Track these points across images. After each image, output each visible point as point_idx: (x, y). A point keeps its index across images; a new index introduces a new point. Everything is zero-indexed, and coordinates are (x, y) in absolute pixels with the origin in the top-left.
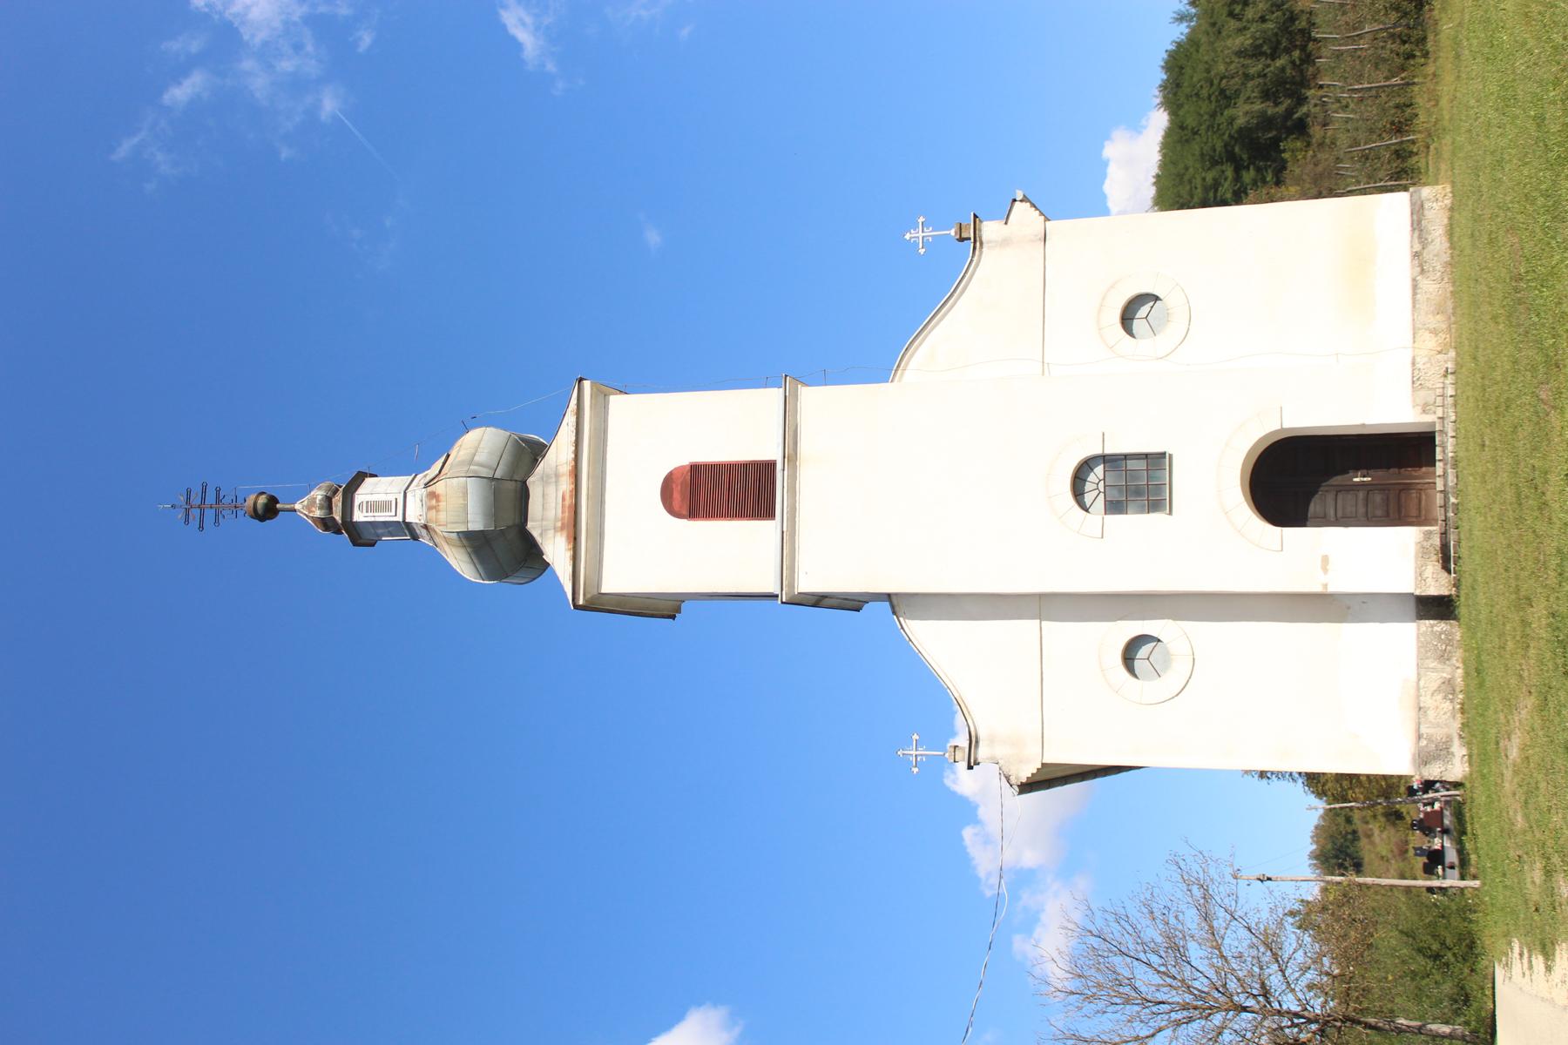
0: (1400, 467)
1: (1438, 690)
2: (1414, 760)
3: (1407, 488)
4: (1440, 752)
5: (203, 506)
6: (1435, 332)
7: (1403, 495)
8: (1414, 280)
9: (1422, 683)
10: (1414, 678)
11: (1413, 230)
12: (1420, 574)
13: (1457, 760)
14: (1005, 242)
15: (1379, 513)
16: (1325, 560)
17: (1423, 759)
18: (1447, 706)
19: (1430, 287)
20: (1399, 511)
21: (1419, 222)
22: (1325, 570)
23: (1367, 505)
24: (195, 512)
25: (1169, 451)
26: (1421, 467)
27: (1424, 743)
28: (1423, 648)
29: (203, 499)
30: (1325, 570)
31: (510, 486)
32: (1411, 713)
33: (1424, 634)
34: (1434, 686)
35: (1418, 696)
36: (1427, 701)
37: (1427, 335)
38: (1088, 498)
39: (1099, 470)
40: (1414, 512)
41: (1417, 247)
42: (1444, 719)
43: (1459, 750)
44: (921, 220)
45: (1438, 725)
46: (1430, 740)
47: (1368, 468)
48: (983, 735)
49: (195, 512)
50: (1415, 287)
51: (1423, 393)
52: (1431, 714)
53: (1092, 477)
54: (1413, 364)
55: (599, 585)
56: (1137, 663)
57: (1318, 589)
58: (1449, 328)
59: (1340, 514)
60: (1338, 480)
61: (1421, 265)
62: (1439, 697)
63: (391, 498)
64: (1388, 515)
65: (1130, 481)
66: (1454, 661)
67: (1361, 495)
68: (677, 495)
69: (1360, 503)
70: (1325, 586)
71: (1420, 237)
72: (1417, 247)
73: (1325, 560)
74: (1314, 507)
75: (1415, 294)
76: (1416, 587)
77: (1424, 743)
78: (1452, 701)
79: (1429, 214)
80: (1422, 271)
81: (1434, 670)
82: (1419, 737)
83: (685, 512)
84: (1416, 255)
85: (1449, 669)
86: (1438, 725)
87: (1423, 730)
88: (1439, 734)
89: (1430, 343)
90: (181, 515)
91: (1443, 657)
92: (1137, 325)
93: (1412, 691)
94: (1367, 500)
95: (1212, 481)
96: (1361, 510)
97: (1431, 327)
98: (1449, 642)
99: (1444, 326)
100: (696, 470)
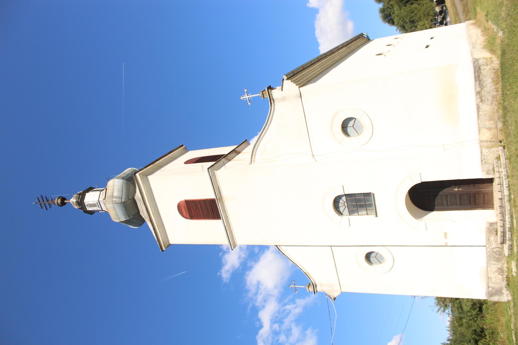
4: (499, 292)
5: (44, 202)
6: (489, 129)
8: (478, 105)
9: (489, 269)
10: (485, 266)
11: (476, 80)
12: (488, 240)
13: (505, 295)
14: (284, 99)
16: (446, 234)
17: (491, 294)
18: (500, 277)
19: (486, 108)
20: (475, 202)
21: (479, 77)
22: (446, 238)
23: (461, 200)
24: (43, 205)
25: (372, 192)
27: (490, 289)
29: (44, 201)
30: (446, 238)
31: (130, 202)
33: (489, 252)
34: (495, 270)
36: (491, 275)
37: (485, 131)
38: (341, 209)
39: (344, 198)
41: (478, 89)
43: (505, 291)
44: (246, 90)
45: (496, 283)
46: (493, 288)
48: (317, 283)
49: (43, 205)
50: (478, 108)
52: (493, 280)
53: (341, 201)
54: (481, 153)
55: (168, 242)
56: (371, 259)
58: (497, 127)
59: (449, 203)
61: (481, 98)
62: (497, 274)
63: (96, 203)
64: (470, 203)
65: (359, 203)
66: (503, 261)
67: (458, 196)
68: (184, 211)
71: (479, 84)
72: (478, 89)
73: (446, 234)
74: (437, 201)
75: (478, 112)
77: (490, 289)
78: (502, 275)
79: (483, 72)
80: (482, 101)
81: (494, 264)
82: (489, 287)
83: (189, 217)
84: (478, 93)
85: (500, 264)
86: (496, 283)
87: (490, 285)
88: (497, 286)
90: (39, 206)
92: (350, 130)
95: (393, 199)
96: (458, 202)
97: (488, 127)
99: (494, 126)
100: (187, 202)
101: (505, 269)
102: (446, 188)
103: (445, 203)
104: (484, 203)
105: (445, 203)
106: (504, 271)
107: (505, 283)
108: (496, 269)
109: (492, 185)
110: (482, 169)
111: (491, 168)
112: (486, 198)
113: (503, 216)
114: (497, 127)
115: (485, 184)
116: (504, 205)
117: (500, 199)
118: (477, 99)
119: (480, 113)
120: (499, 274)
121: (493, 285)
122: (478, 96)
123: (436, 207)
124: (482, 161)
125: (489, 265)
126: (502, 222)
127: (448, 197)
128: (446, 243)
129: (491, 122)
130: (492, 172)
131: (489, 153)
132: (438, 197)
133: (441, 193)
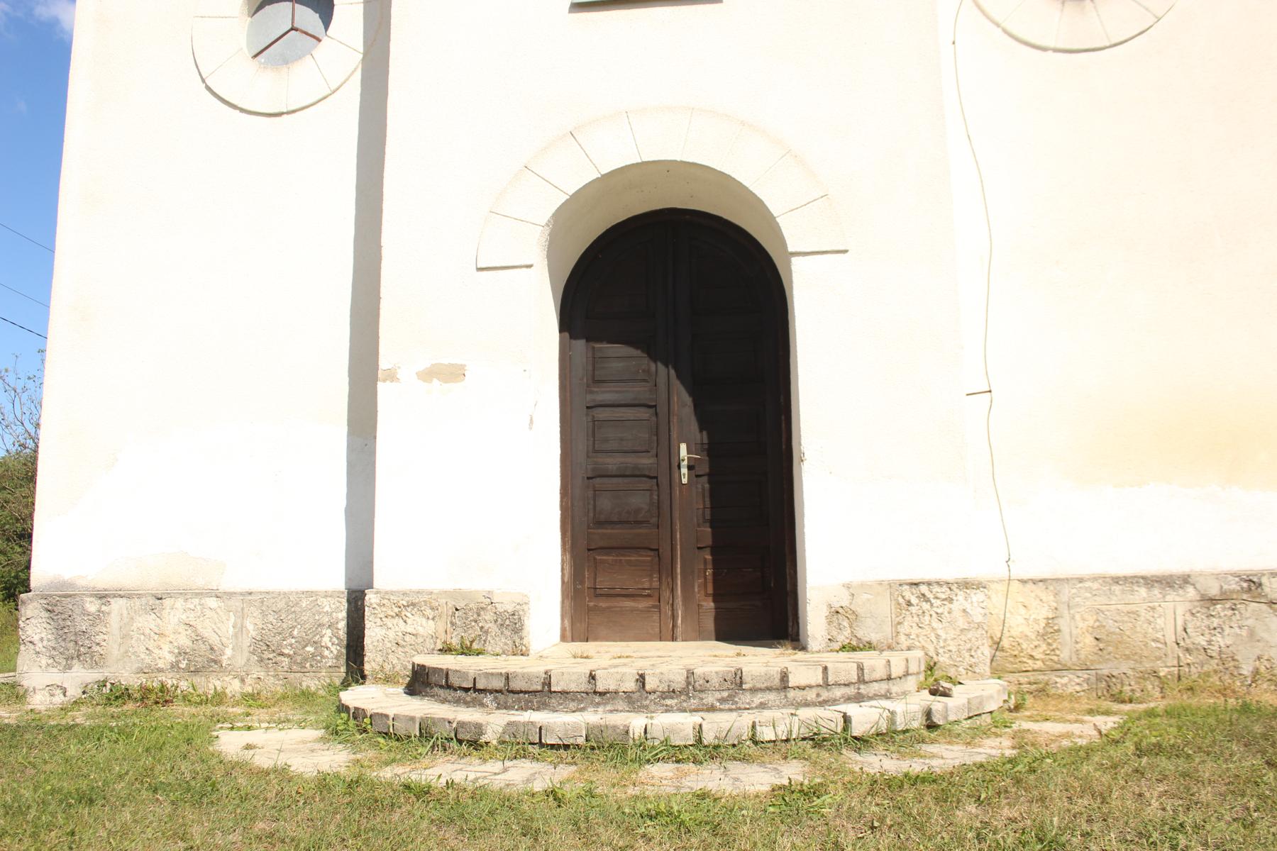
0: (714, 550)
1: (198, 638)
2: (64, 585)
3: (663, 567)
4: (74, 643)
6: (1050, 631)
7: (646, 557)
8: (1186, 580)
9: (212, 602)
10: (233, 581)
12: (410, 604)
13: (56, 677)
15: (605, 503)
16: (454, 373)
17: (60, 606)
18: (165, 656)
19: (1169, 617)
22: (429, 374)
26: (717, 597)
27: (92, 606)
28: (282, 608)
30: (429, 374)
32: (154, 582)
34: (207, 631)
35: (185, 594)
36: (175, 613)
37: (1044, 613)
40: (604, 582)
42: (138, 649)
43: (78, 678)
46: (99, 617)
47: (711, 475)
50: (1167, 582)
51: (885, 607)
52: (147, 622)
54: (966, 585)
57: (384, 363)
58: (1061, 669)
59: (603, 414)
60: (682, 401)
61: (1224, 597)
62: (184, 641)
64: (599, 524)
66: (258, 672)
67: (646, 461)
69: (631, 460)
70: (392, 376)
73: (454, 373)
74: (620, 356)
75: (1150, 581)
76: (385, 595)
78: (174, 666)
81: (240, 629)
82: (103, 596)
85: (240, 661)
87: (117, 605)
88: (110, 641)
89: (1022, 620)
91: (265, 650)
93: (200, 582)
94: (637, 474)
96: (612, 462)
97: (1063, 624)
98: (301, 664)
99: (1065, 655)
101: (212, 684)
102: (697, 406)
103: (605, 394)
104: (597, 593)
105: (605, 394)
106: (197, 680)
107: (129, 678)
108: (214, 639)
109: (701, 636)
110: (863, 586)
111: (868, 632)
112: (628, 604)
113: (672, 693)
114: (1061, 669)
115: (710, 604)
116: (744, 699)
117: (784, 677)
118: (1217, 576)
119: (1143, 591)
120: (182, 653)
121: (114, 621)
122: (1233, 585)
123: (580, 344)
124: (929, 584)
125: (236, 603)
126: (630, 685)
127: (644, 414)
128: (392, 376)
129: (1089, 640)
130: (843, 638)
131: (962, 623)
132: (646, 362)
133: (663, 372)
